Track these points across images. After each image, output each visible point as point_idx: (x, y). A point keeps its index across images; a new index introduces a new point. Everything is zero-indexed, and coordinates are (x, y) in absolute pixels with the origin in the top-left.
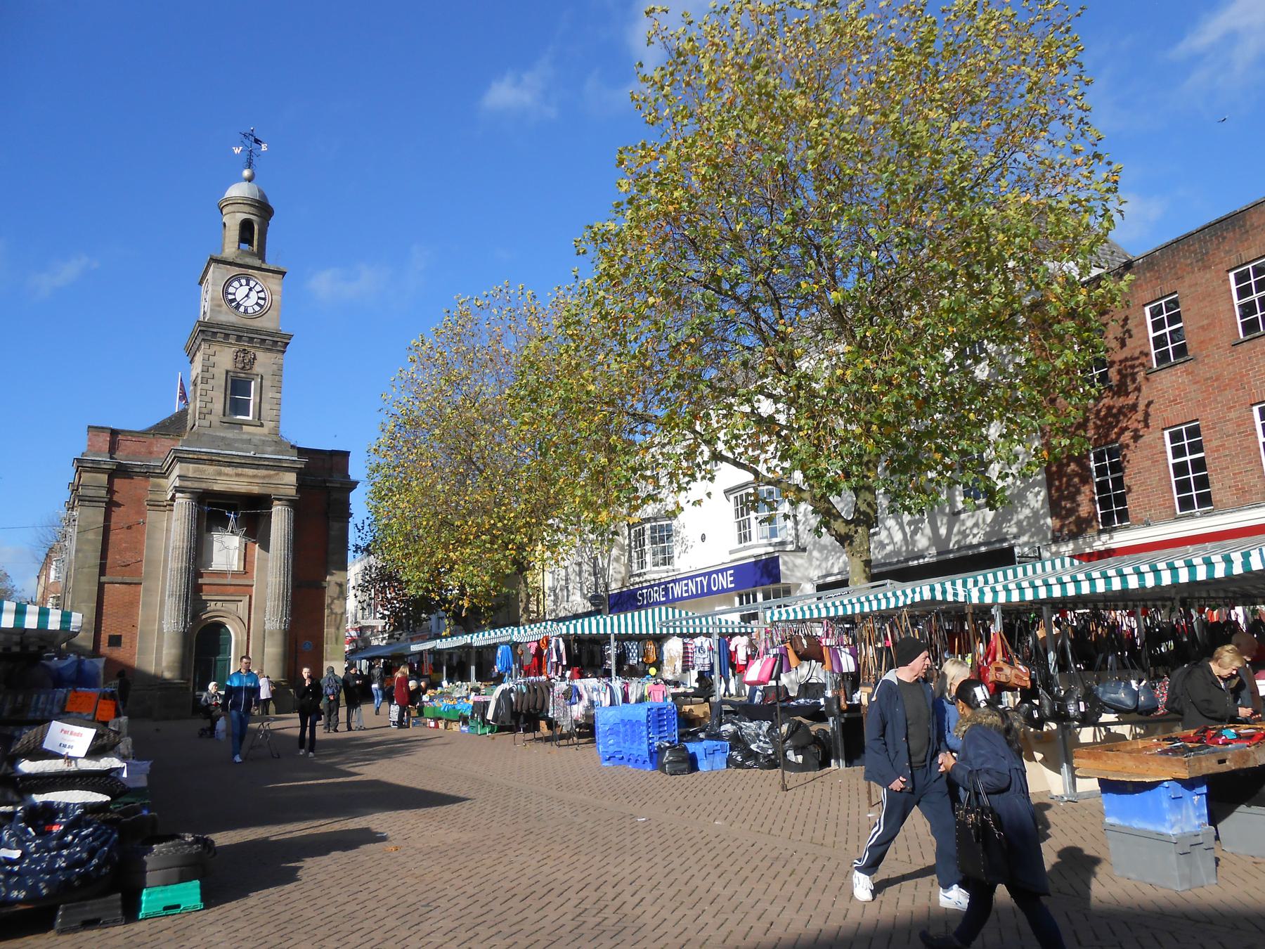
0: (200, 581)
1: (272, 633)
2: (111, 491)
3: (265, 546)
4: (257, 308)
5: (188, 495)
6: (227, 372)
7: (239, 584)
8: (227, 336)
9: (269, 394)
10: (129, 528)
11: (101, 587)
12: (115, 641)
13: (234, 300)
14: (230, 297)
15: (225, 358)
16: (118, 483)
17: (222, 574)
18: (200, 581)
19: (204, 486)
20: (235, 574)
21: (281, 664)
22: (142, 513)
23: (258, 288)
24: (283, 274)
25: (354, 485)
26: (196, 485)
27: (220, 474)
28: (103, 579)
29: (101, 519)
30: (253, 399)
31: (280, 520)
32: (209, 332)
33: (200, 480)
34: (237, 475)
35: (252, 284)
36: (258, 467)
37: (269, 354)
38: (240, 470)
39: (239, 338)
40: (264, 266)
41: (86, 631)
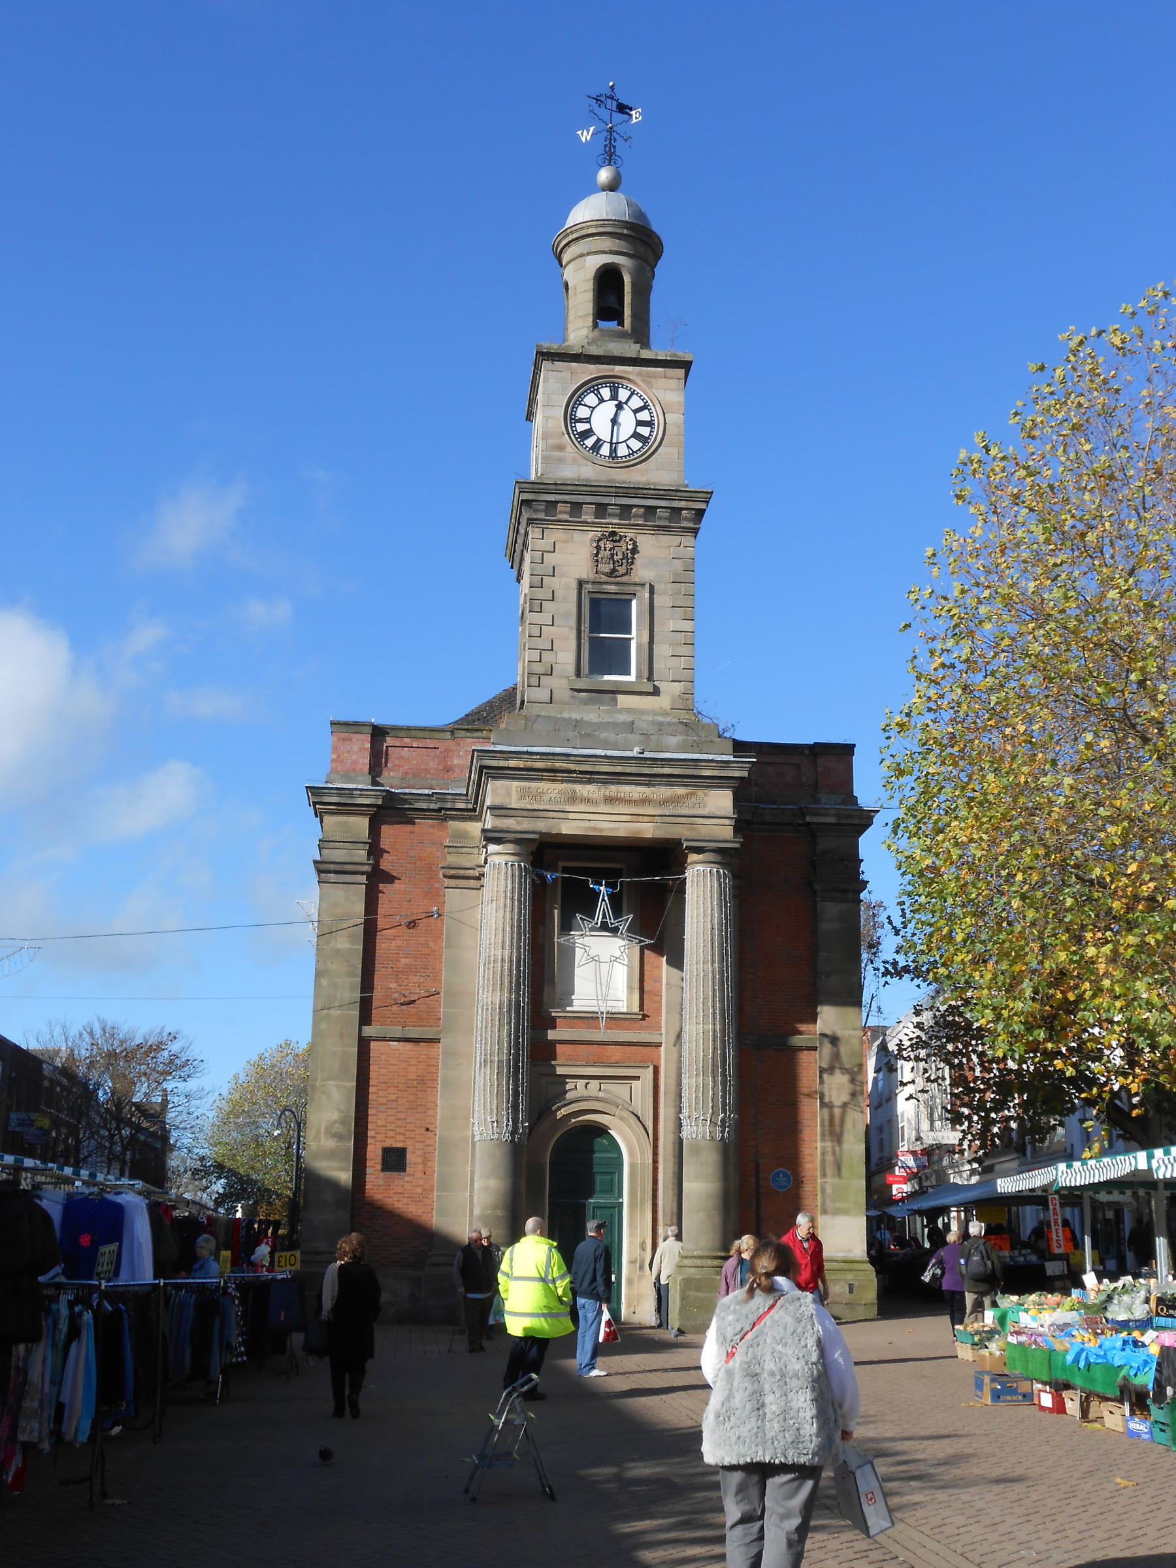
0: (552, 1035)
1: (696, 1150)
2: (375, 850)
4: (636, 444)
5: (510, 848)
6: (581, 583)
7: (630, 1041)
8: (576, 507)
9: (668, 623)
10: (412, 925)
11: (364, 1045)
12: (395, 1160)
13: (588, 433)
14: (581, 427)
15: (572, 554)
16: (389, 834)
18: (552, 1035)
19: (542, 826)
20: (615, 1019)
21: (717, 1220)
22: (435, 894)
23: (636, 402)
24: (686, 365)
25: (864, 820)
26: (526, 825)
27: (573, 798)
28: (368, 1031)
29: (360, 908)
30: (636, 636)
31: (702, 894)
32: (540, 503)
33: (532, 813)
34: (609, 800)
35: (623, 394)
36: (650, 780)
38: (613, 790)
39: (601, 510)
40: (645, 354)
41: (340, 1137)
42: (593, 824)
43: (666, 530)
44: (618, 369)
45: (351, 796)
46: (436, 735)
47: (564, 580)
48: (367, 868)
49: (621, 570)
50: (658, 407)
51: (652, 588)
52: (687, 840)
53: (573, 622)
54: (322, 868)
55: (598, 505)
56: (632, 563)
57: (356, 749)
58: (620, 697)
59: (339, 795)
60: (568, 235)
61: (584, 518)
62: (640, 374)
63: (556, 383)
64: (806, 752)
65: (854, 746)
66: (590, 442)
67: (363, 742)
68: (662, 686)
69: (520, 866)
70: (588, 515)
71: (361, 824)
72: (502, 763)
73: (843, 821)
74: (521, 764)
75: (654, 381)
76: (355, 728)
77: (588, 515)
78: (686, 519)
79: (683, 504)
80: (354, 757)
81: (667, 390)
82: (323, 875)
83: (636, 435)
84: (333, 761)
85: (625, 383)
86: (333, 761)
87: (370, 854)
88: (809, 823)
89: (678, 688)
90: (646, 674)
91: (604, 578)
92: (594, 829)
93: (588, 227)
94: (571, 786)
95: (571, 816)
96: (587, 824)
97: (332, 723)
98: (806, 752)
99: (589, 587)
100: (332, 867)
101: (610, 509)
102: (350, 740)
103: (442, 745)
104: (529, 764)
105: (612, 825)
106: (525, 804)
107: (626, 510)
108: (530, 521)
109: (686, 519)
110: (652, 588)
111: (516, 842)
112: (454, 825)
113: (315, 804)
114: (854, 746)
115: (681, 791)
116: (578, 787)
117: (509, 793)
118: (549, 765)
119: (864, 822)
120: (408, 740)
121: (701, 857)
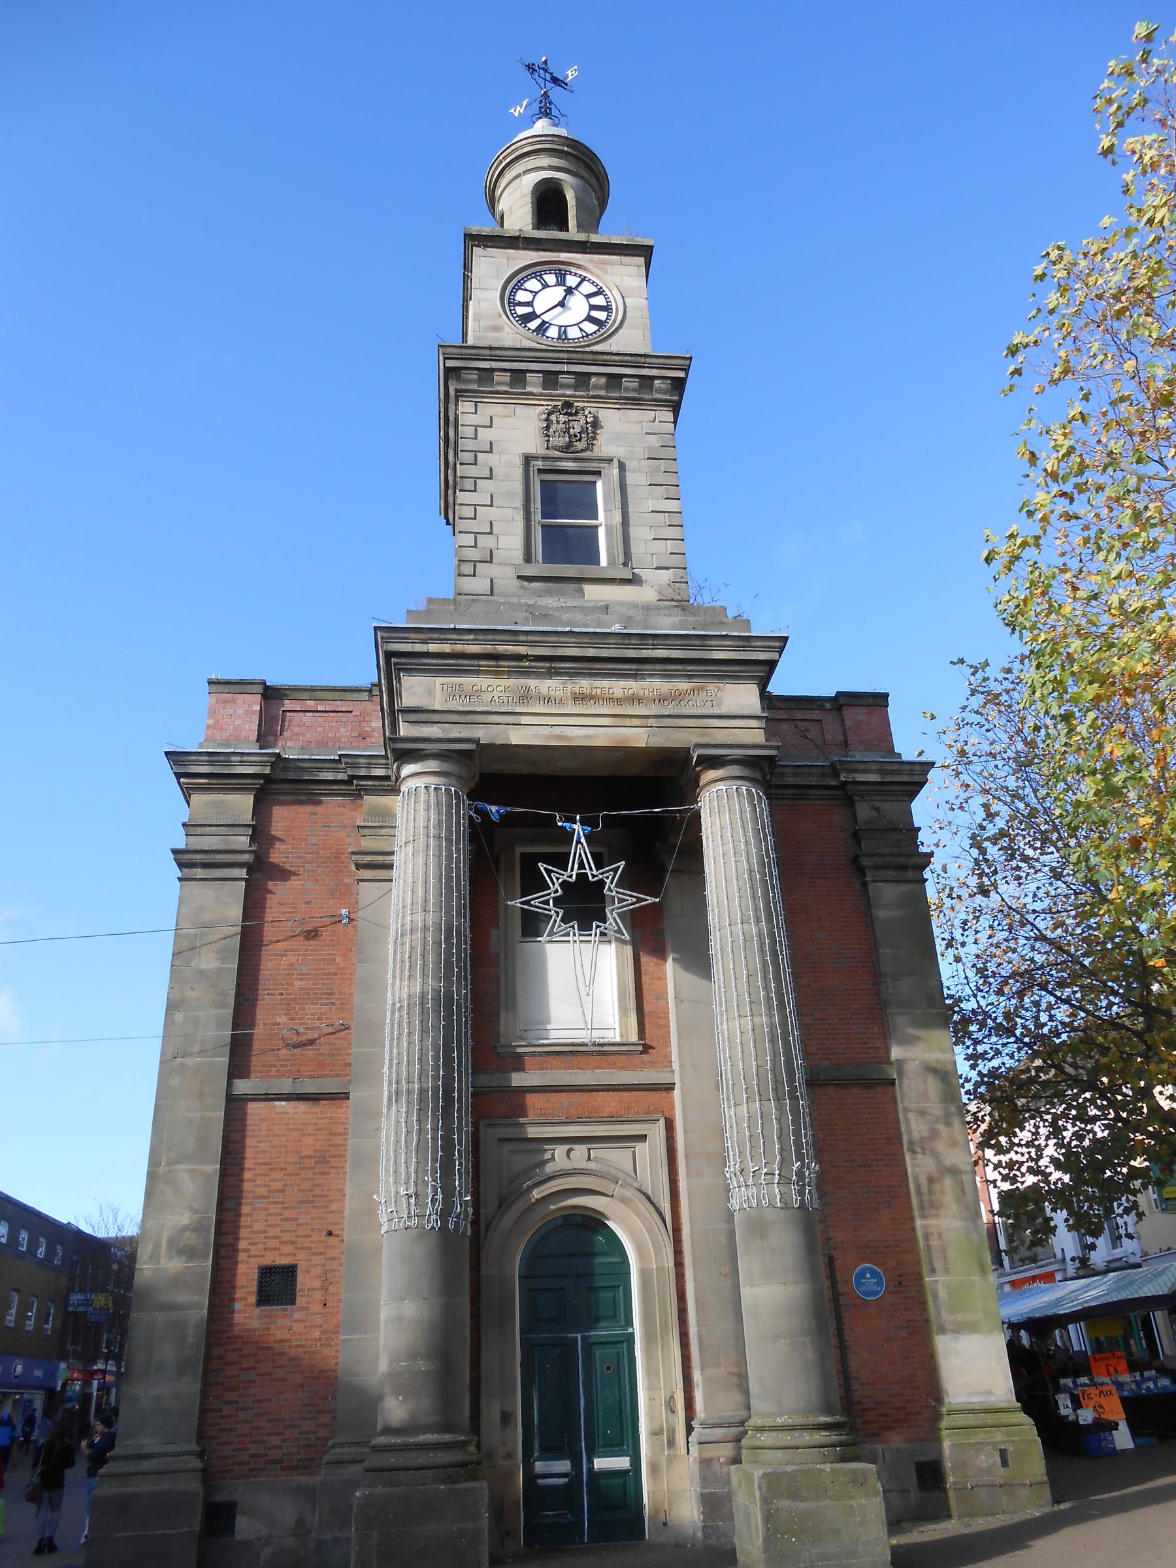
1: (758, 1227)
2: (259, 831)
3: (698, 960)
4: (590, 328)
5: (433, 765)
6: (528, 459)
8: (518, 377)
9: (645, 502)
10: (312, 934)
11: (235, 1106)
12: (278, 1285)
13: (532, 316)
14: (521, 311)
15: (512, 431)
16: (282, 817)
17: (573, 1054)
19: (484, 734)
21: (810, 1354)
22: (344, 893)
23: (587, 288)
24: (645, 252)
25: (911, 779)
26: (456, 732)
27: (525, 697)
28: (242, 1086)
29: (235, 912)
30: (605, 519)
31: (728, 827)
32: (468, 373)
33: (466, 716)
34: (579, 698)
35: (571, 281)
36: (636, 667)
37: (634, 415)
38: (584, 685)
39: (551, 379)
40: (594, 238)
41: (190, 1253)
42: (557, 731)
43: (634, 402)
44: (564, 256)
45: (228, 763)
46: (348, 696)
47: (504, 457)
48: (247, 858)
49: (580, 445)
50: (616, 292)
51: (622, 467)
52: (698, 746)
53: (519, 502)
54: (184, 860)
55: (545, 373)
56: (594, 438)
57: (240, 712)
58: (588, 589)
59: (211, 763)
60: (501, 162)
61: (528, 389)
62: (591, 261)
63: (492, 268)
64: (828, 705)
65: (887, 695)
66: (534, 325)
67: (254, 703)
68: (645, 574)
69: (448, 791)
70: (534, 384)
71: (242, 804)
72: (419, 648)
73: (888, 779)
74: (447, 648)
75: (608, 268)
76: (240, 688)
77: (534, 384)
78: (660, 391)
79: (654, 372)
80: (238, 722)
81: (622, 279)
82: (186, 870)
83: (590, 319)
84: (208, 727)
85: (573, 270)
86: (208, 727)
87: (253, 839)
88: (845, 783)
89: (666, 576)
90: (621, 560)
91: (557, 454)
92: (560, 737)
93: (522, 147)
94: (522, 681)
95: (524, 720)
96: (549, 730)
97: (210, 683)
98: (828, 705)
99: (540, 464)
100: (198, 858)
101: (562, 379)
102: (234, 701)
103: (357, 709)
104: (459, 648)
105: (585, 731)
106: (457, 705)
107: (582, 380)
108: (460, 393)
109: (660, 391)
110: (622, 467)
111: (440, 756)
112: (370, 800)
113: (178, 776)
114: (887, 695)
115: (683, 685)
116: (533, 683)
117: (430, 693)
118: (488, 648)
119: (916, 779)
120: (311, 703)
121: (720, 773)
